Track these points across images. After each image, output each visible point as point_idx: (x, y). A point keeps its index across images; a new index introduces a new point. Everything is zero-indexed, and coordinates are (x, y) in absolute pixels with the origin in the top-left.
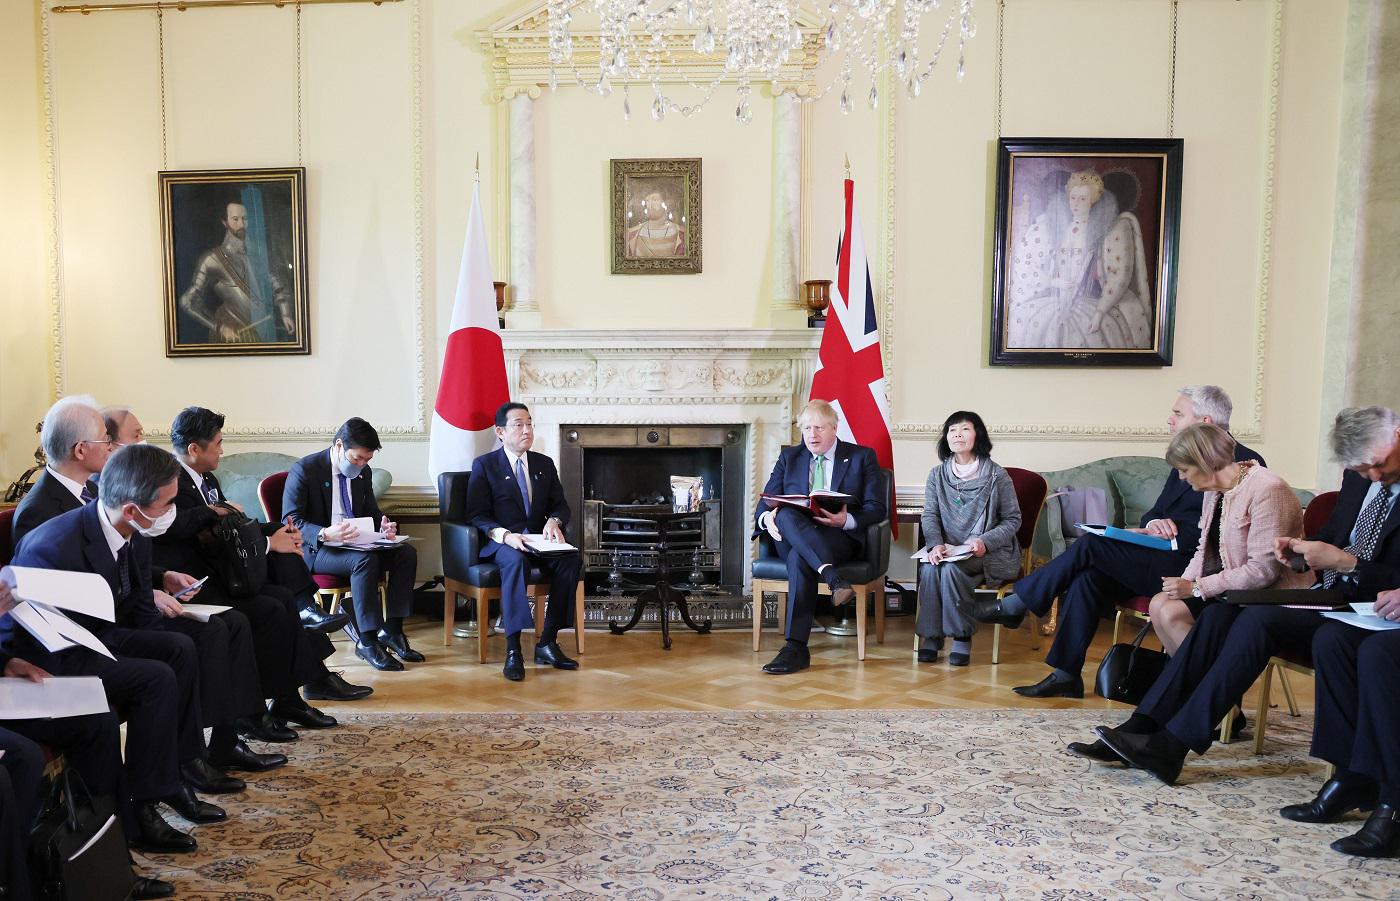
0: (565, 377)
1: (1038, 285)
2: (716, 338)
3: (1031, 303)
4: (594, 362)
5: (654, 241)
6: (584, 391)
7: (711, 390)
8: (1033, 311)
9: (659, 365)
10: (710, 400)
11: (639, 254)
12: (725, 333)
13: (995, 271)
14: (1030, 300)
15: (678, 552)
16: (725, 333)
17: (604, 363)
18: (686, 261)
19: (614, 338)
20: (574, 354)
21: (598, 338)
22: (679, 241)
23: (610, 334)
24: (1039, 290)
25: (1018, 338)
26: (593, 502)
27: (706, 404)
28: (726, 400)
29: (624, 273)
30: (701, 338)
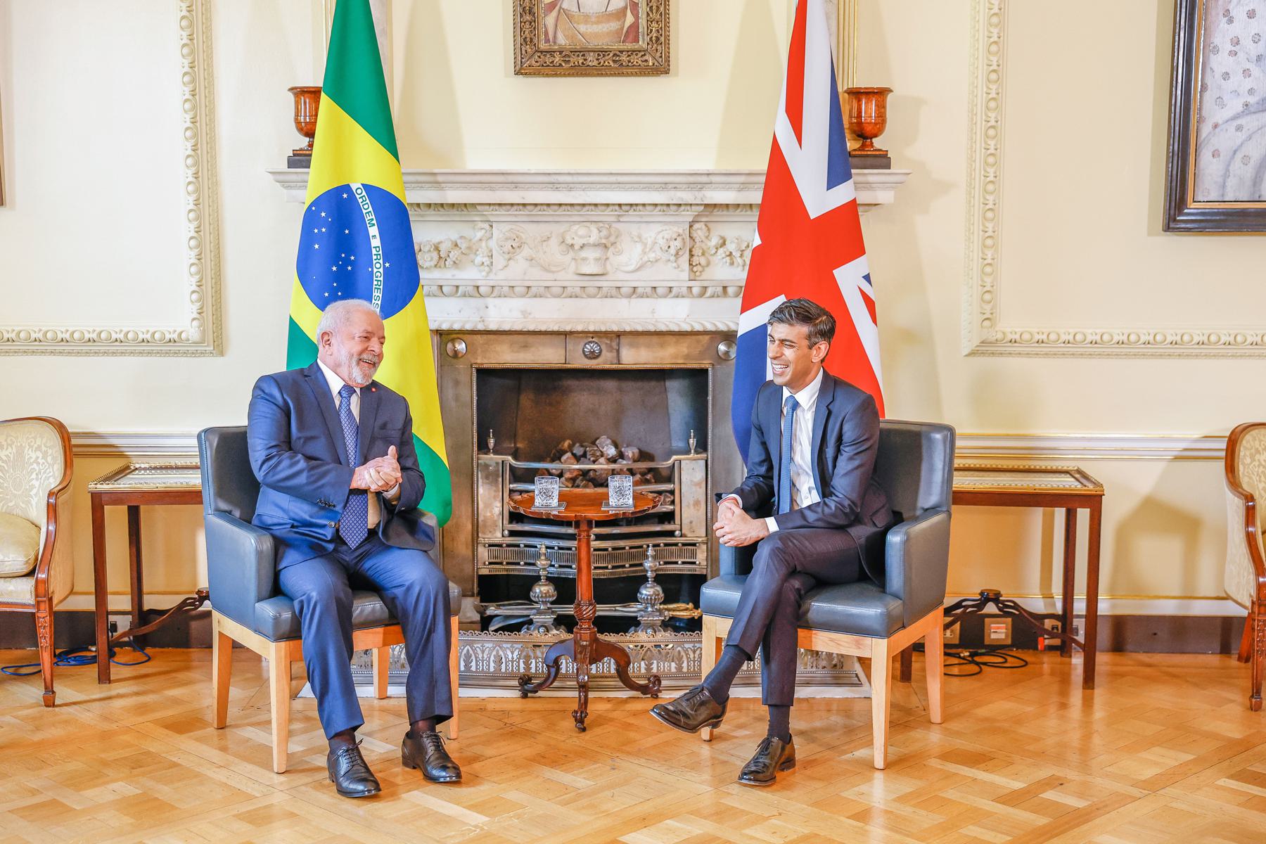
0: (437, 249)
1: (1251, 92)
2: (691, 186)
3: (1239, 122)
4: (486, 226)
5: (586, 19)
7: (685, 275)
8: (1241, 136)
9: (595, 231)
10: (684, 290)
11: (562, 40)
12: (704, 179)
13: (1174, 69)
14: (1234, 118)
15: (621, 543)
16: (704, 179)
18: (641, 52)
19: (516, 185)
21: (489, 186)
22: (630, 19)
23: (510, 178)
24: (1252, 100)
25: (1216, 182)
26: (492, 459)
30: (665, 186)
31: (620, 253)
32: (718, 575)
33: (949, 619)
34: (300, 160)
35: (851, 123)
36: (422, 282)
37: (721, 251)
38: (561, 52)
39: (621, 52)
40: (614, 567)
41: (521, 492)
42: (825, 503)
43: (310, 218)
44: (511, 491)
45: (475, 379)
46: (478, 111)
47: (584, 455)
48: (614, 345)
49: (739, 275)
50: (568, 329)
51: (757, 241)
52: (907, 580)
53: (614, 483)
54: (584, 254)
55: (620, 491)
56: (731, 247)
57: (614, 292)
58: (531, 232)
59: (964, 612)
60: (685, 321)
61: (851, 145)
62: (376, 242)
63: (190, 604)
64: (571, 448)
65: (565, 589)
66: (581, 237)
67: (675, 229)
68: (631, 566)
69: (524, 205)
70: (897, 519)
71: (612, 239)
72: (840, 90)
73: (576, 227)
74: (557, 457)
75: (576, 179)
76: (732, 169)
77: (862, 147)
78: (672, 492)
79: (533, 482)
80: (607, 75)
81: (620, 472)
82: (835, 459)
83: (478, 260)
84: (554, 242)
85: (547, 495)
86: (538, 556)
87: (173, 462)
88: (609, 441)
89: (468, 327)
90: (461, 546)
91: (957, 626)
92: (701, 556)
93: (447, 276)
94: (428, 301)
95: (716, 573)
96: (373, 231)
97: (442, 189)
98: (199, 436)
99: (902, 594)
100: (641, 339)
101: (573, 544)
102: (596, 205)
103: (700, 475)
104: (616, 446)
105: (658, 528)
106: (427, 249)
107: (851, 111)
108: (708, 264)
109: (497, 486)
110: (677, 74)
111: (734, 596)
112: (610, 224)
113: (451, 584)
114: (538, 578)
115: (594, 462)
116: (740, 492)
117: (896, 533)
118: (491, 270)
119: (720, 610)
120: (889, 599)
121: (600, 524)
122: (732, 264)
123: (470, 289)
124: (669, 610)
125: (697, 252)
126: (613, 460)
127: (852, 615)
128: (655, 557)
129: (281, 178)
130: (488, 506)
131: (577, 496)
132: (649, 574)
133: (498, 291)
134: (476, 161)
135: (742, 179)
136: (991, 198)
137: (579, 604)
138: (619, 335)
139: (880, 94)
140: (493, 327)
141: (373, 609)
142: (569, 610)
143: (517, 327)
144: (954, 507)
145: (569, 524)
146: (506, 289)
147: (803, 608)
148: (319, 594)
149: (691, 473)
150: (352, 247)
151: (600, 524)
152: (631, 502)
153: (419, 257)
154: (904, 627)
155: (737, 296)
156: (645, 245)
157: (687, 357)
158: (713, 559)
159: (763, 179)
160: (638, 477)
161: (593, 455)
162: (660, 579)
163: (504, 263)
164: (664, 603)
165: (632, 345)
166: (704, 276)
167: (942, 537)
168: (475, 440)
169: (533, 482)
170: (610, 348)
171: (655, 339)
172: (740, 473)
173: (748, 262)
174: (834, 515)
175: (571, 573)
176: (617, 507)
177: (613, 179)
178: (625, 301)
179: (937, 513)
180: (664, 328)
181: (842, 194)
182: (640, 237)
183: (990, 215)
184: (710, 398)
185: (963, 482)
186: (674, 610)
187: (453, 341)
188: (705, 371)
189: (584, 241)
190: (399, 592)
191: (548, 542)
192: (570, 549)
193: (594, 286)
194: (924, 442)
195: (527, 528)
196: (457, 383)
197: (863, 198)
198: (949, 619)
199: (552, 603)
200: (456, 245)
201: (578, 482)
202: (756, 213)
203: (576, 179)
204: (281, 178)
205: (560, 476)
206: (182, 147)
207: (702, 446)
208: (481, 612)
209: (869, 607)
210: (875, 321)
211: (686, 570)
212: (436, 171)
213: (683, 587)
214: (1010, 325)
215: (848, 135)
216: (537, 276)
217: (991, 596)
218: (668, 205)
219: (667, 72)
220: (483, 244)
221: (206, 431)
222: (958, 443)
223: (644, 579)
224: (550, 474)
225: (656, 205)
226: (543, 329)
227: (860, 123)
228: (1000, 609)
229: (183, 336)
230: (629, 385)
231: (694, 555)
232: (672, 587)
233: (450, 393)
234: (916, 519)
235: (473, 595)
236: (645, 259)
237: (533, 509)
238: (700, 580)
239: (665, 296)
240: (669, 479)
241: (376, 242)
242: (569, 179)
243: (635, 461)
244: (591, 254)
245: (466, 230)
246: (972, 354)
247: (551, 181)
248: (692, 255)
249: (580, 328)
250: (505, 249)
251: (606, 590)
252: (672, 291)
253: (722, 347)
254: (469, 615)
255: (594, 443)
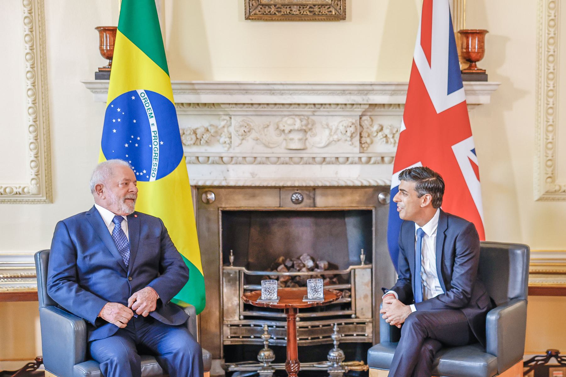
0: (195, 132)
4: (227, 118)
6: (216, 149)
7: (357, 150)
15: (316, 323)
17: (239, 119)
20: (206, 108)
26: (232, 269)
27: (352, 163)
28: (373, 160)
29: (259, 19)
31: (315, 135)
32: (379, 342)
33: (527, 369)
34: (103, 74)
35: (462, 52)
36: (185, 155)
37: (380, 134)
38: (275, 6)
39: (315, 5)
40: (312, 339)
41: (251, 291)
42: (448, 295)
43: (110, 112)
44: (245, 290)
45: (220, 217)
46: (221, 44)
47: (293, 266)
48: (311, 194)
49: (392, 149)
50: (281, 184)
51: (403, 128)
52: (500, 344)
53: (311, 284)
54: (291, 136)
55: (315, 290)
56: (386, 131)
57: (311, 160)
58: (257, 122)
59: (536, 364)
60: (357, 179)
61: (463, 66)
62: (154, 128)
63: (31, 367)
64: (284, 262)
65: (280, 353)
66: (289, 125)
67: (350, 120)
68: (324, 337)
69: (252, 104)
70: (493, 305)
71: (310, 126)
72: (455, 31)
73: (286, 119)
74: (275, 268)
75: (285, 87)
76: (387, 81)
77: (470, 68)
78: (350, 290)
79: (260, 284)
80: (305, 20)
81: (316, 277)
82: (452, 266)
83: (222, 140)
84: (272, 129)
85: (269, 293)
86: (262, 332)
87: (19, 274)
88: (308, 257)
89: (216, 184)
90: (213, 327)
91: (532, 373)
92: (369, 331)
93: (202, 150)
94: (188, 166)
95: (378, 341)
96: (152, 121)
97: (198, 94)
98: (36, 256)
99: (496, 353)
100: (329, 191)
101: (285, 324)
102: (299, 104)
103: (368, 278)
104: (313, 260)
105: (340, 313)
106: (189, 132)
107: (462, 45)
108: (372, 143)
109: (236, 287)
110: (350, 20)
111: (389, 355)
112: (308, 117)
113: (204, 351)
114: (261, 347)
115: (299, 271)
116: (396, 289)
117: (493, 314)
118: (230, 147)
119: (380, 365)
120: (488, 356)
121: (302, 310)
122: (387, 142)
123: (217, 159)
124: (348, 366)
125: (364, 134)
126: (311, 269)
127: (465, 367)
128: (339, 332)
129: (91, 86)
130: (230, 299)
131: (288, 292)
132: (335, 343)
133: (235, 159)
134: (221, 75)
135: (393, 88)
136: (551, 100)
137: (289, 363)
138: (314, 188)
139: (480, 34)
140: (232, 184)
141: (153, 369)
142: (282, 366)
143: (248, 184)
144: (529, 298)
145: (280, 310)
146: (240, 159)
147: (435, 363)
148: (118, 359)
149: (362, 277)
150: (139, 133)
151: (302, 310)
152: (322, 296)
153: (183, 138)
154: (498, 374)
155: (390, 163)
156: (331, 130)
157: (359, 202)
158: (376, 333)
159: (406, 88)
160: (328, 280)
161: (299, 266)
162: (342, 346)
163: (239, 142)
164: (345, 361)
165: (323, 195)
166: (370, 150)
167: (522, 316)
168: (221, 257)
169: (260, 284)
170: (309, 197)
171: (338, 191)
172: (394, 277)
173: (397, 141)
174: (453, 302)
175: (284, 342)
176: (313, 299)
177: (309, 87)
178: (318, 167)
179: (519, 301)
180: (342, 184)
181: (457, 97)
182: (327, 125)
183: (550, 111)
184: (374, 229)
185: (534, 281)
186: (351, 366)
187: (206, 193)
188: (370, 212)
189: (292, 128)
190: (169, 357)
191: (269, 323)
192: (283, 327)
193: (297, 157)
194: (511, 256)
195: (255, 314)
196: (208, 220)
197: (471, 100)
198: (527, 369)
199: (272, 362)
200: (208, 130)
201: (289, 284)
202: (402, 110)
203: (285, 87)
204: (91, 86)
205: (277, 279)
206: (23, 66)
207: (369, 260)
208: (226, 368)
209: (475, 361)
210: (478, 179)
211: (359, 339)
212: (194, 82)
213: (357, 351)
214: (565, 181)
215: (460, 59)
216: (261, 151)
217: (553, 354)
218: (346, 104)
219: (344, 18)
220: (226, 130)
221: (40, 252)
222: (532, 256)
223: (331, 346)
224: (270, 278)
225: (338, 104)
226: (265, 184)
227: (468, 52)
228: (559, 362)
229: (26, 190)
230: (323, 221)
231: (363, 330)
232: (350, 350)
233: (204, 226)
234: (506, 304)
235: (220, 358)
236: (331, 139)
237: (258, 301)
238: (367, 346)
239: (344, 163)
240: (348, 281)
241: (154, 128)
242: (281, 87)
243: (325, 270)
244: (296, 136)
245: (215, 121)
246: (540, 199)
247: (270, 88)
248: (361, 136)
249: (289, 184)
250: (240, 134)
251: (305, 354)
252: (349, 161)
253: (381, 196)
254: (217, 371)
255: (299, 258)
